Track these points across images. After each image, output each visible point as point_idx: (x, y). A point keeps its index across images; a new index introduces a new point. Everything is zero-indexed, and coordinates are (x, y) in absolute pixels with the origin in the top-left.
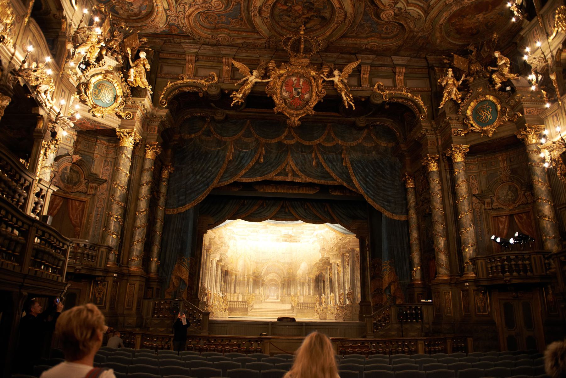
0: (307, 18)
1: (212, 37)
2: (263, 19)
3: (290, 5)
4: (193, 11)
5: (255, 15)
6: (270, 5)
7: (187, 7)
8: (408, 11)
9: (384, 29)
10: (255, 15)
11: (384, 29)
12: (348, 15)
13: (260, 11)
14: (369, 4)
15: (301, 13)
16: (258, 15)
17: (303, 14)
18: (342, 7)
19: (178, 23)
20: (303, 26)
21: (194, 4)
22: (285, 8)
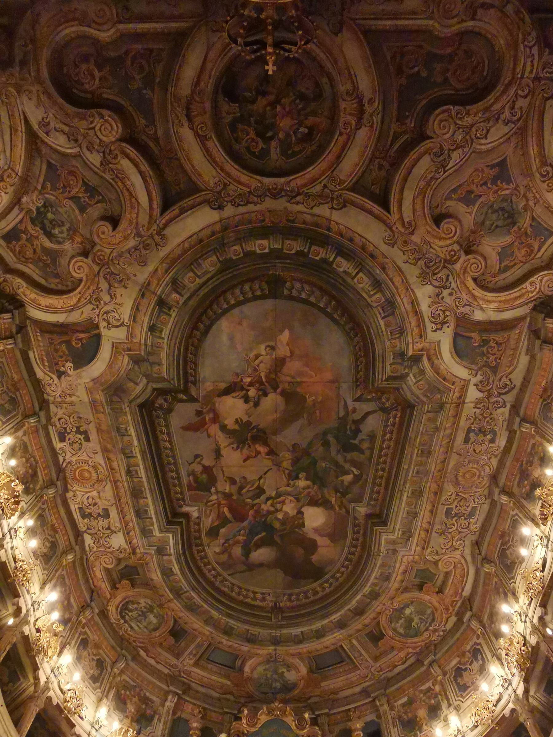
0: (264, 94)
1: (475, 13)
2: (355, 87)
3: (302, 130)
4: (497, 99)
5: (371, 101)
6: (341, 134)
7: (507, 114)
8: (73, 144)
9: (97, 73)
10: (371, 101)
11: (97, 73)
12: (186, 125)
13: (360, 113)
14: (151, 144)
15: (279, 108)
16: (365, 101)
17: (273, 105)
18: (202, 139)
19: (540, 58)
20: (270, 72)
21: (491, 123)
22: (311, 120)
